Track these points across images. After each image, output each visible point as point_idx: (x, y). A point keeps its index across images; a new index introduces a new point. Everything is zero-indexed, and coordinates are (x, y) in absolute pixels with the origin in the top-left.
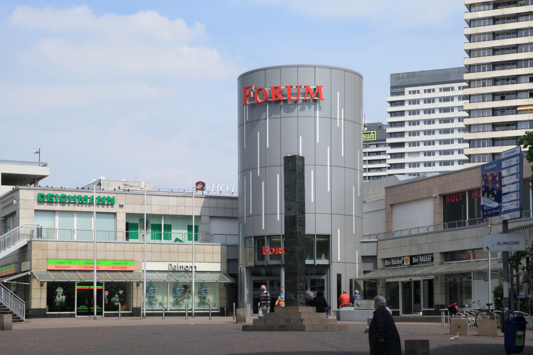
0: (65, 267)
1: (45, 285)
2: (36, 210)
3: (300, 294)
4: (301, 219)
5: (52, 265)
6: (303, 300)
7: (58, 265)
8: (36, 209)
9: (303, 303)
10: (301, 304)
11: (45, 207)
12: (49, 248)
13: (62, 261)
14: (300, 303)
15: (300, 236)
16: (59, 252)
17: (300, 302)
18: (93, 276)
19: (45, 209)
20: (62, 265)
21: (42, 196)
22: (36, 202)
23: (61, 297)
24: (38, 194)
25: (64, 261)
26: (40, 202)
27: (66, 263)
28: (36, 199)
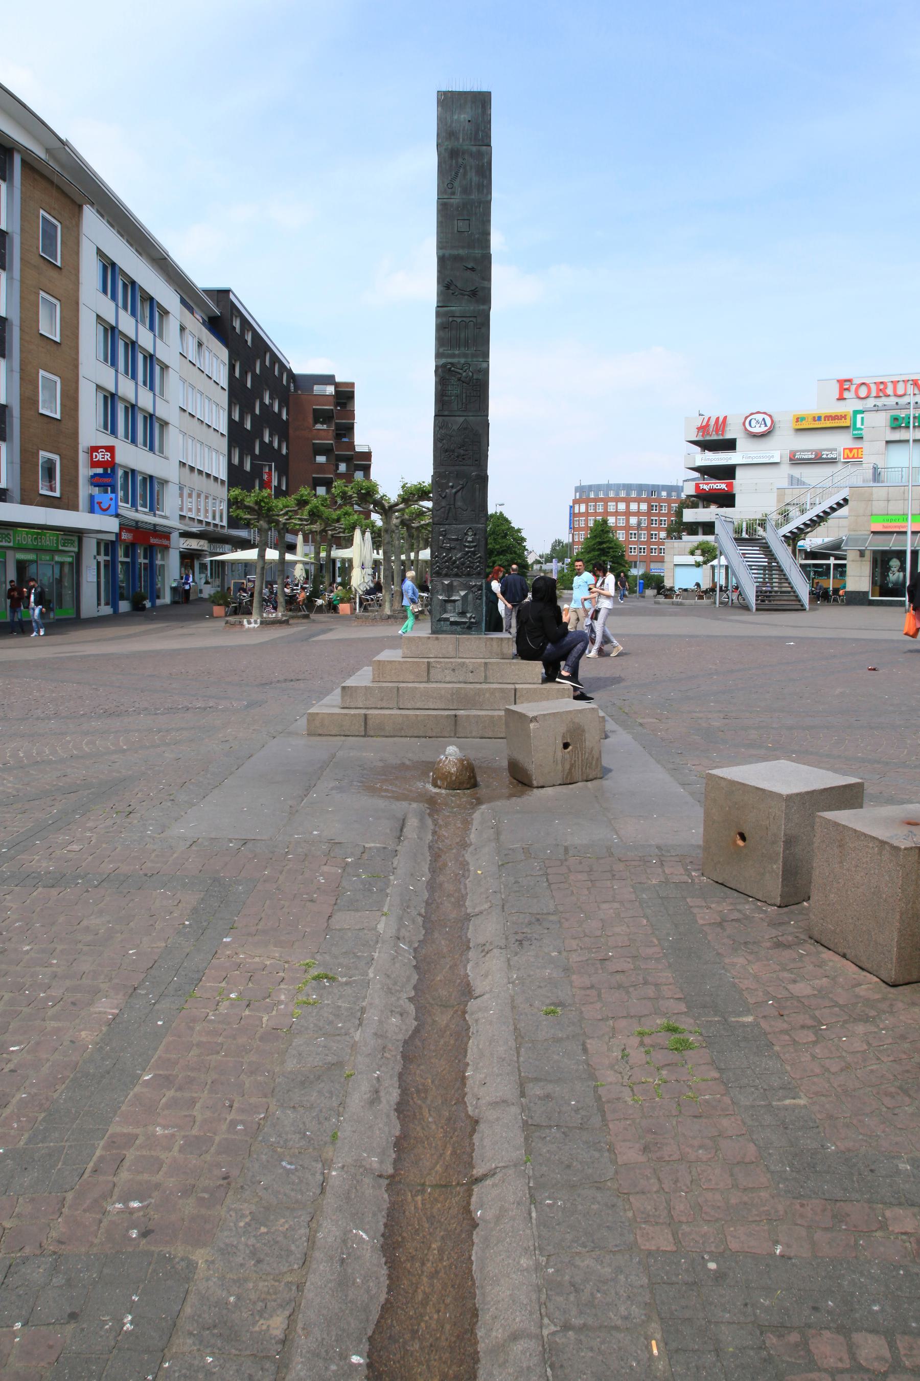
0: (899, 527)
1: (868, 555)
2: (888, 442)
3: (450, 589)
4: (459, 320)
5: (878, 524)
6: (463, 614)
7: (886, 523)
8: (888, 439)
9: (465, 623)
10: (458, 628)
11: (897, 436)
12: (875, 497)
13: (893, 517)
14: (448, 623)
15: (454, 380)
16: (891, 503)
17: (447, 619)
18: (906, 541)
19: (902, 438)
20: (894, 523)
21: (896, 419)
22: (888, 430)
23: (897, 574)
24: (891, 416)
25: (897, 517)
26: (893, 428)
27: (901, 520)
28: (888, 424)
